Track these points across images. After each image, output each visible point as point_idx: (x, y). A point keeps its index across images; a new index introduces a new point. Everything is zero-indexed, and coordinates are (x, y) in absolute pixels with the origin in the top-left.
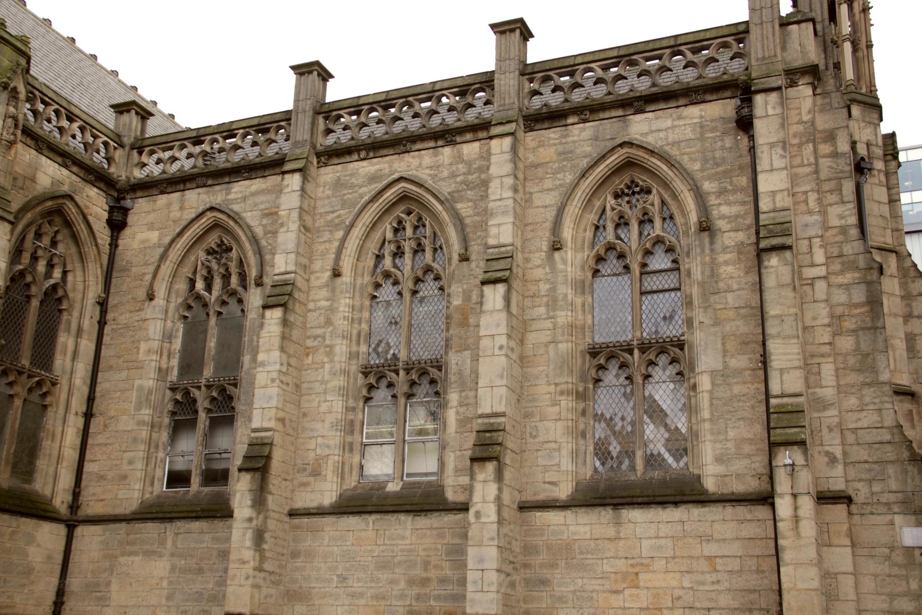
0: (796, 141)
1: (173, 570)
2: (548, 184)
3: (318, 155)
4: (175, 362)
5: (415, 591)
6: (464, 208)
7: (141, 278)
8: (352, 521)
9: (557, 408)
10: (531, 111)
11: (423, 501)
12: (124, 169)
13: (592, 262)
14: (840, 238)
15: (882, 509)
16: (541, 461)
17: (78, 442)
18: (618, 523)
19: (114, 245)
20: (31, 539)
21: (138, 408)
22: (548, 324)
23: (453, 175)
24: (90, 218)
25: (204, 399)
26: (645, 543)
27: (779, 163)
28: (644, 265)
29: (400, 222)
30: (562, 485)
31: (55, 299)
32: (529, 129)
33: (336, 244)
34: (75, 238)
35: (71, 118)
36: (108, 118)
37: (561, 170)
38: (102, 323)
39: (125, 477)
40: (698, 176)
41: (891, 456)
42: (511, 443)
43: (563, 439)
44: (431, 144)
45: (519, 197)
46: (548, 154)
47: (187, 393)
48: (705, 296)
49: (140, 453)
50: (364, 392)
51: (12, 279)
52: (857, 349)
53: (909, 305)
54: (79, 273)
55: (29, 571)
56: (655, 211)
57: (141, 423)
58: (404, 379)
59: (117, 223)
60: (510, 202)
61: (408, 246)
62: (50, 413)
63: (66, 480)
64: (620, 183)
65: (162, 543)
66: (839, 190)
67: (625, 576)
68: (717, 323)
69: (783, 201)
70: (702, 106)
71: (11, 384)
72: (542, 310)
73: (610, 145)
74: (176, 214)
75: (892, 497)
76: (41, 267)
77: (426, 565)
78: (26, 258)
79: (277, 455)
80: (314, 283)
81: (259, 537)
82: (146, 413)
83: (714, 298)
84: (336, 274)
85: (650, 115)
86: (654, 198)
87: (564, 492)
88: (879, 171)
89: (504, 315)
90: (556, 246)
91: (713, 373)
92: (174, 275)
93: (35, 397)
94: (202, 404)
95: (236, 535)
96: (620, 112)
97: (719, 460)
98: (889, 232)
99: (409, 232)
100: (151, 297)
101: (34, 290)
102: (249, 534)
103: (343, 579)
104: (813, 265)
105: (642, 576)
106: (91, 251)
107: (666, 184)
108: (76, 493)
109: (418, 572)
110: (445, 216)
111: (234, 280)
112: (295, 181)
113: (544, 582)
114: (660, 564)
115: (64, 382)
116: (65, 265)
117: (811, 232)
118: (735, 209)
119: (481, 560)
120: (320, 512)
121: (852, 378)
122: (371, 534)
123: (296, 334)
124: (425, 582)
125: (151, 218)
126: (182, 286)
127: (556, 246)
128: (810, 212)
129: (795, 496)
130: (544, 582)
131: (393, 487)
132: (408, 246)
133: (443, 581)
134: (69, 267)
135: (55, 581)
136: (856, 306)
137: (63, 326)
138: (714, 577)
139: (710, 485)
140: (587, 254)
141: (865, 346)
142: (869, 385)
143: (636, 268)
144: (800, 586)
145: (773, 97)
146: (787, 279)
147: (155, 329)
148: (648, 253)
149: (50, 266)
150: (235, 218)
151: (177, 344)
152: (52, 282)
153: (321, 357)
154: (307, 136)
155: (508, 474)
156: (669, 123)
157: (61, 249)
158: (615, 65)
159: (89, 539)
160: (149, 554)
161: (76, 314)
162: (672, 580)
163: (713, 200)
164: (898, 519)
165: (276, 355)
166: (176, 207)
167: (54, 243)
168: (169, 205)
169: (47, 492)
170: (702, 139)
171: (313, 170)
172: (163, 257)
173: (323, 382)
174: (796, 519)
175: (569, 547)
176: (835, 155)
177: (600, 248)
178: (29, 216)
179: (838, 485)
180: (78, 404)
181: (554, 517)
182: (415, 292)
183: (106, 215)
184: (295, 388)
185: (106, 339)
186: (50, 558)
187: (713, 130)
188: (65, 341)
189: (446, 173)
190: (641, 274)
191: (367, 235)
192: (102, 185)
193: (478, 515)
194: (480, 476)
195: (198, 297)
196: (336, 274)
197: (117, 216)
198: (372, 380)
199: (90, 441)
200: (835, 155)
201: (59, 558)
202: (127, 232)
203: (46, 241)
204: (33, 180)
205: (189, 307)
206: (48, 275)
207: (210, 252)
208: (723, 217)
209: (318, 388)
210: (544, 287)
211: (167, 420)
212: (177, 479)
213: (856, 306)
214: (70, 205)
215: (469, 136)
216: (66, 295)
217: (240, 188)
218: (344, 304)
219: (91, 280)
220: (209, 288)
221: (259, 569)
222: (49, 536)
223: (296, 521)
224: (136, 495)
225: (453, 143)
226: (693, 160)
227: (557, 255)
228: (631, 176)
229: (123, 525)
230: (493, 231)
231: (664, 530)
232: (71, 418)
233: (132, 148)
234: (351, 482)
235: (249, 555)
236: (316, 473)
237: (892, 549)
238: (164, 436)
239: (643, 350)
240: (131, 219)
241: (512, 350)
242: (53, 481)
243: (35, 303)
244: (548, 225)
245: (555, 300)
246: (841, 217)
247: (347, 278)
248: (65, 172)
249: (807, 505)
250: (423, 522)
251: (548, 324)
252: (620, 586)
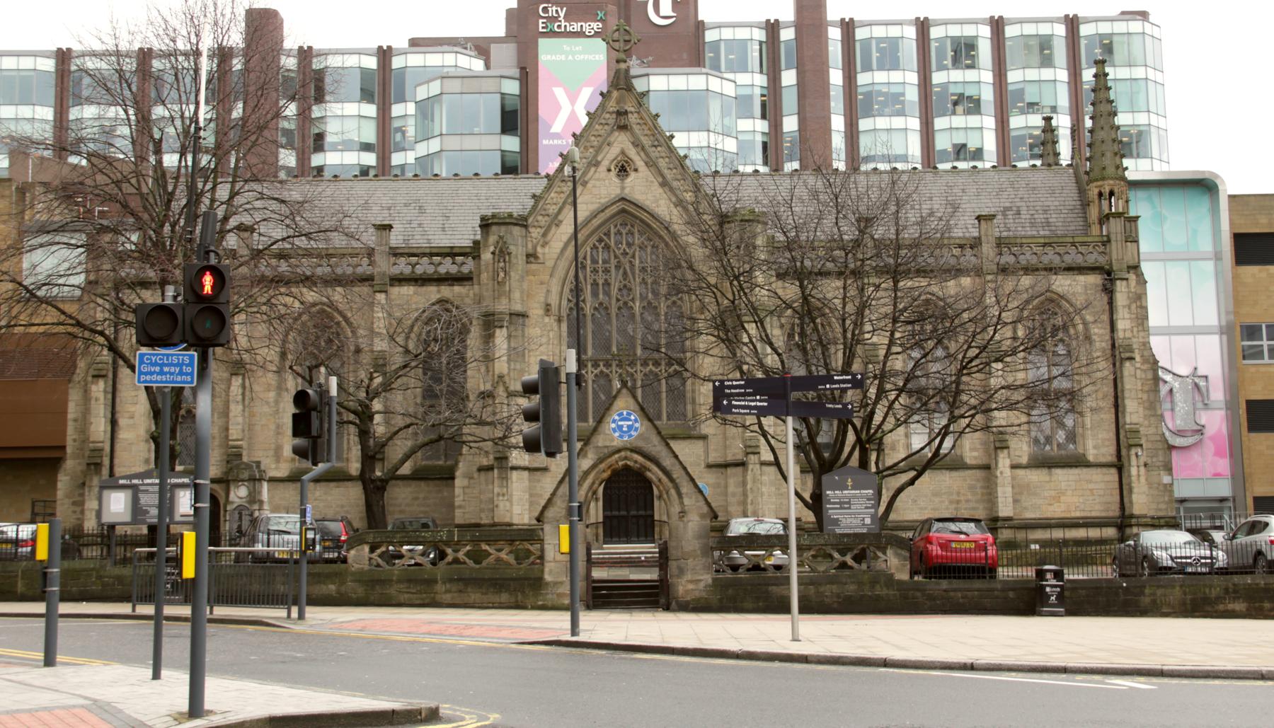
5: (954, 506)
18: (1050, 475)
27: (1127, 316)
67: (1054, 498)
69: (1128, 334)
77: (958, 494)
97: (1095, 447)
109: (955, 497)
114: (1069, 493)
118: (1101, 331)
121: (1147, 412)
124: (958, 502)
133: (967, 501)
141: (1152, 398)
145: (1124, 283)
156: (1068, 282)
162: (1075, 499)
174: (1139, 475)
231: (1071, 478)
249: (1142, 469)
250: (955, 474)
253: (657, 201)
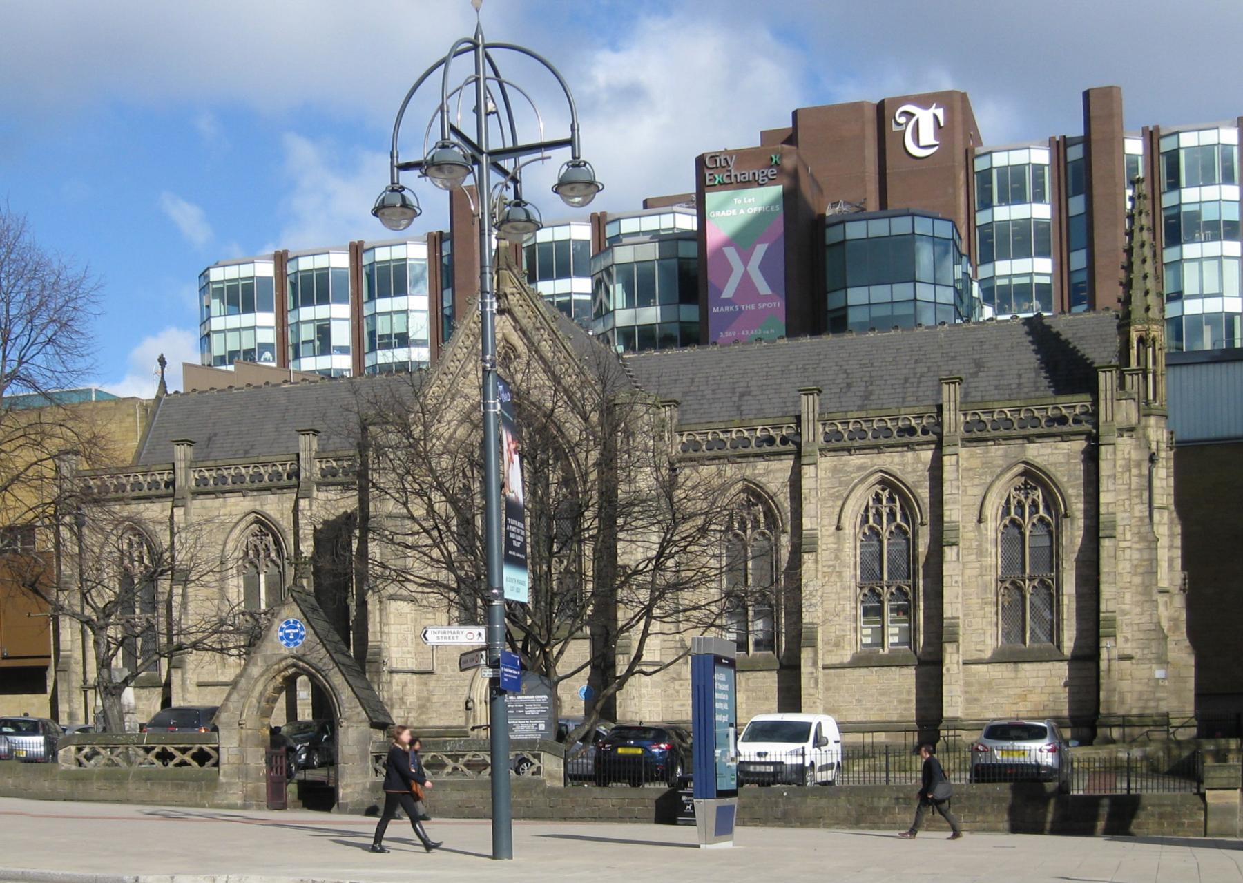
18: (1016, 670)
23: (914, 471)
37: (984, 474)
52: (1143, 583)
67: (1020, 696)
72: (973, 557)
73: (1014, 461)
96: (1020, 441)
120: (842, 666)
121: (1140, 598)
122: (875, 677)
156: (1049, 451)
170: (1068, 463)
175: (990, 682)
179: (1128, 652)
189: (910, 469)
198: (866, 591)
210: (975, 544)
223: (827, 671)
225: (913, 450)
231: (1041, 674)
251: (977, 565)
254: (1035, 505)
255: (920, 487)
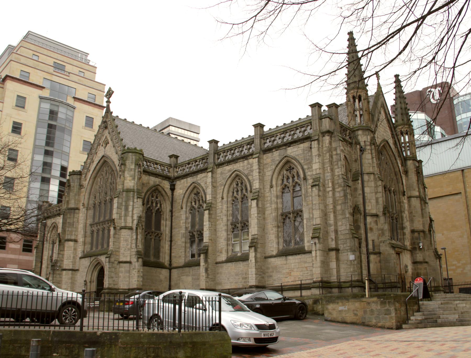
0: (325, 152)
1: (192, 279)
2: (269, 169)
3: (216, 165)
4: (190, 225)
5: (244, 281)
6: (250, 177)
7: (179, 203)
8: (229, 264)
9: (272, 231)
10: (264, 149)
11: (245, 258)
12: (172, 174)
13: (281, 190)
14: (338, 178)
15: (346, 251)
16: (270, 245)
17: (169, 248)
19: (173, 195)
20: (160, 273)
21: (182, 238)
22: (270, 208)
23: (248, 168)
24: (165, 189)
25: (195, 236)
26: (292, 265)
27: (317, 161)
28: (294, 190)
29: (237, 182)
30: (274, 251)
31: (159, 213)
32: (264, 154)
33: (222, 190)
34: (162, 195)
35: (157, 164)
36: (167, 160)
37: (272, 165)
38: (172, 216)
39: (180, 256)
40: (303, 164)
41: (348, 237)
42: (259, 242)
43: (274, 239)
44: (242, 160)
45: (261, 174)
46: (269, 160)
47: (193, 233)
48: (305, 198)
49: (183, 250)
50: (232, 230)
51: (147, 209)
52: (341, 209)
53: (377, 189)
54: (164, 204)
55: (161, 281)
56: (295, 174)
57: (183, 242)
58: (239, 226)
59: (173, 189)
60: (258, 176)
61: (239, 189)
62: (162, 242)
63: (167, 258)
64: (287, 167)
65: (190, 273)
66: (337, 164)
67: (288, 273)
68: (308, 205)
70: (304, 144)
71: (150, 236)
72: (269, 205)
74: (186, 185)
75: (348, 248)
76: (154, 205)
78: (150, 203)
79: (210, 249)
80: (218, 201)
81: (206, 270)
82: (183, 240)
83: (307, 198)
84: (223, 198)
85: (292, 147)
86: (295, 170)
87: (275, 253)
88: (368, 149)
89: (256, 208)
90: (271, 187)
91: (307, 219)
92: (187, 202)
93: (157, 238)
94: (196, 236)
95: (201, 269)
97: (308, 242)
98: (371, 168)
99: (240, 185)
100: (182, 208)
101: (153, 211)
102: (204, 269)
103: (228, 279)
104: (329, 187)
105: (292, 273)
106: (167, 198)
107: (296, 167)
108: (170, 262)
109: (244, 276)
110: (246, 180)
111: (201, 201)
112: (210, 174)
113: (271, 276)
115: (164, 233)
116: (160, 202)
117: (329, 178)
119: (252, 272)
120: (223, 262)
122: (234, 267)
123: (213, 216)
124: (246, 278)
125: (180, 186)
126: (189, 204)
127: (271, 187)
128: (328, 173)
129: (316, 251)
130: (271, 276)
131: (239, 254)
132: (239, 189)
134: (162, 203)
135: (168, 283)
136: (341, 197)
137: (162, 219)
138: (306, 272)
139: (306, 248)
140: (279, 188)
142: (343, 218)
143: (292, 191)
144: (317, 272)
145: (316, 142)
146: (317, 194)
147: (183, 217)
148: (294, 186)
149: (157, 204)
150: (199, 184)
151: (190, 220)
152: (157, 208)
153: (220, 221)
154: (213, 161)
155: (259, 250)
156: (296, 149)
157: (159, 198)
158: (283, 133)
159: (174, 272)
160: (187, 275)
161: (165, 215)
163: (306, 171)
164: (349, 253)
165: (208, 223)
166: (186, 183)
167: (157, 198)
168: (184, 182)
169: (163, 261)
170: (304, 153)
171: (215, 170)
172: (184, 197)
173: (221, 228)
174: (316, 256)
176: (337, 154)
177: (283, 186)
178: (149, 193)
180: (168, 238)
181: (272, 260)
182: (242, 202)
183: (169, 187)
184: (214, 230)
185: (173, 221)
186: (166, 277)
187: (306, 151)
188: (163, 222)
189: (246, 168)
190: (293, 192)
191: (230, 187)
192: (167, 179)
193: (251, 261)
194: (251, 251)
195: (193, 207)
196: (223, 198)
197: (172, 187)
198: (233, 227)
199: (172, 248)
200: (337, 154)
201: (168, 278)
202: (175, 191)
203: (155, 197)
204: (149, 183)
205: (192, 210)
206: (156, 206)
207: (195, 194)
208: (309, 175)
209: (220, 230)
210: (269, 198)
211: (189, 241)
212: (193, 256)
213: (341, 197)
214: (159, 187)
215: (250, 157)
216: (162, 210)
217: (200, 176)
218: (225, 206)
219: (168, 206)
220: (195, 204)
221: (207, 277)
222: (164, 273)
223: (217, 265)
224: (183, 261)
225: (247, 159)
226: (302, 160)
227: (272, 189)
228: (288, 165)
229: (181, 269)
230: (254, 185)
231: (297, 261)
232: (167, 242)
233: (174, 167)
234: (230, 254)
235: (204, 274)
236: (221, 252)
237: (347, 261)
238: (188, 245)
239: (293, 213)
240: (176, 187)
241: (260, 217)
242: (165, 259)
243: (154, 214)
244: (269, 181)
245: (272, 202)
246: (338, 172)
247: (225, 199)
248: (157, 179)
251: (270, 208)
252: (287, 276)
253: (112, 154)
254: (293, 177)
255: (250, 175)
